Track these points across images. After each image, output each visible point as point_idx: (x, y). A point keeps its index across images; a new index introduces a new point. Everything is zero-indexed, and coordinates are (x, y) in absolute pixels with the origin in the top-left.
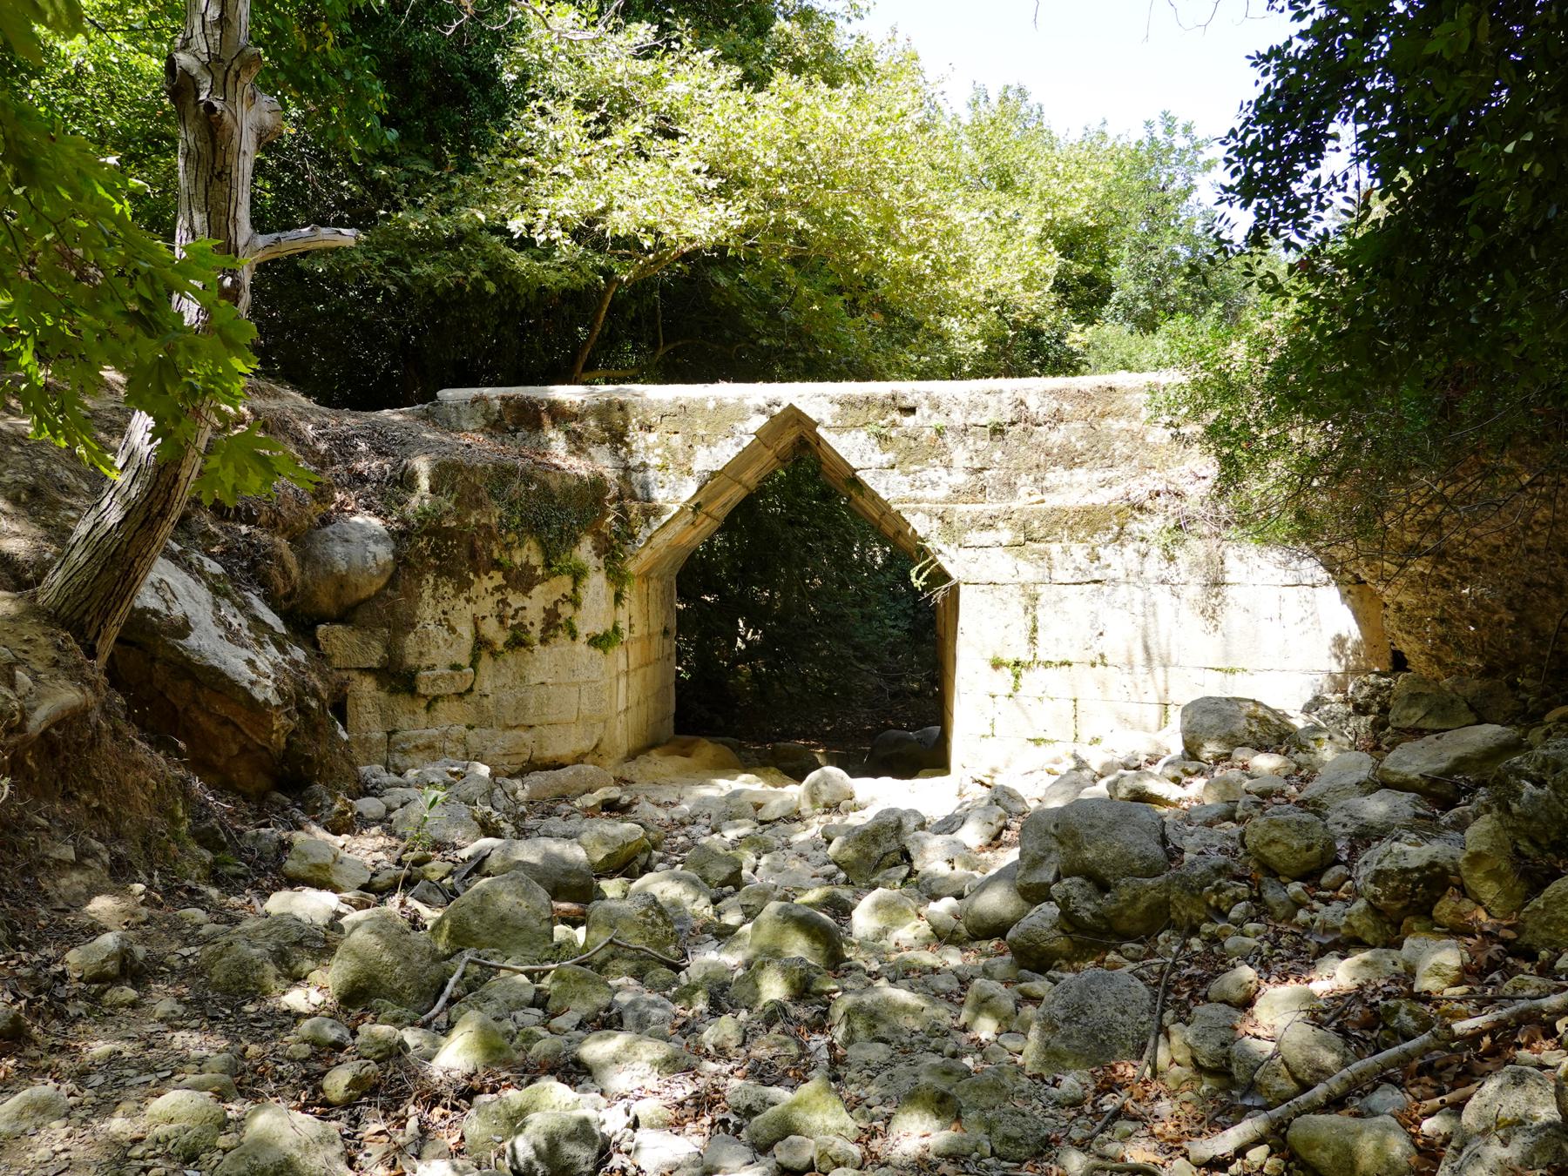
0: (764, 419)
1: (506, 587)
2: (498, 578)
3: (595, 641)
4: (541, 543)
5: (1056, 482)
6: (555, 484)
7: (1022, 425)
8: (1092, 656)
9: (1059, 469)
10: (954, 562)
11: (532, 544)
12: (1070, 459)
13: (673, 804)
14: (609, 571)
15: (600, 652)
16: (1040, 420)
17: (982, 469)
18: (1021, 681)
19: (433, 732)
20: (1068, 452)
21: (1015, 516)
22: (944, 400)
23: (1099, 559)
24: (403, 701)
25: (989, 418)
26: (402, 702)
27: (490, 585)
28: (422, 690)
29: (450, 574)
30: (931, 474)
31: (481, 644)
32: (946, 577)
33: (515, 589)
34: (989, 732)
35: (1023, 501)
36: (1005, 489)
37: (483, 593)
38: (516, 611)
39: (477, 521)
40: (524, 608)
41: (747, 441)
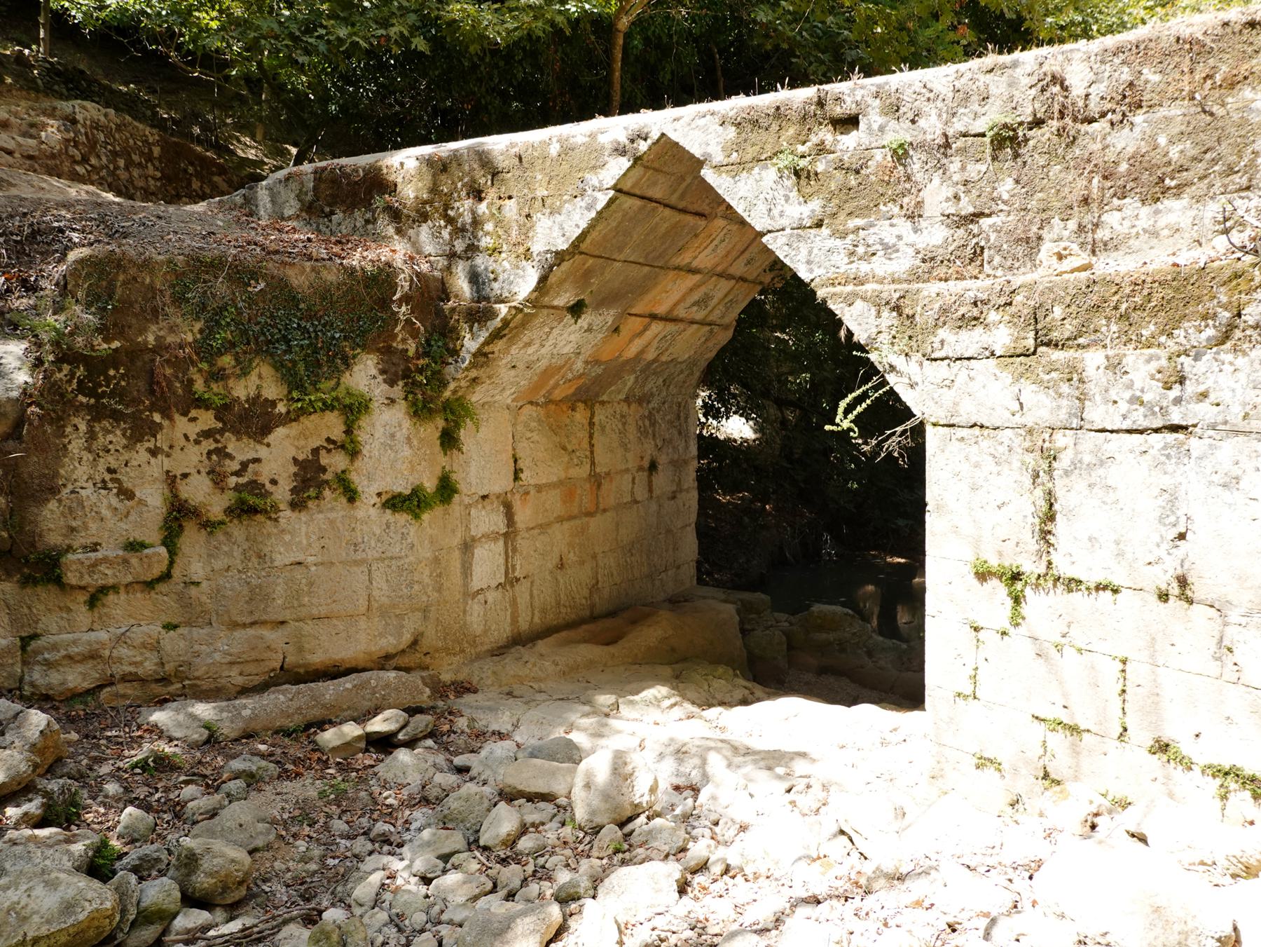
0: (624, 163)
1: (221, 432)
2: (207, 420)
3: (394, 503)
4: (278, 366)
5: (1123, 229)
6: (299, 279)
7: (1055, 124)
8: (1164, 577)
9: (1131, 203)
10: (918, 385)
11: (266, 370)
12: (1155, 182)
13: (501, 736)
14: (414, 404)
15: (402, 518)
16: (1094, 107)
17: (977, 216)
18: (1025, 609)
19: (103, 636)
20: (1150, 169)
21: (1018, 299)
22: (907, 96)
23: (1182, 381)
24: (45, 595)
25: (989, 118)
26: (43, 599)
27: (193, 430)
28: (71, 578)
29: (116, 416)
30: (884, 231)
31: (180, 515)
32: (906, 413)
33: (237, 433)
34: (968, 690)
35: (1054, 266)
36: (1020, 250)
37: (183, 442)
38: (244, 465)
39: (158, 338)
40: (257, 460)
41: (602, 199)
